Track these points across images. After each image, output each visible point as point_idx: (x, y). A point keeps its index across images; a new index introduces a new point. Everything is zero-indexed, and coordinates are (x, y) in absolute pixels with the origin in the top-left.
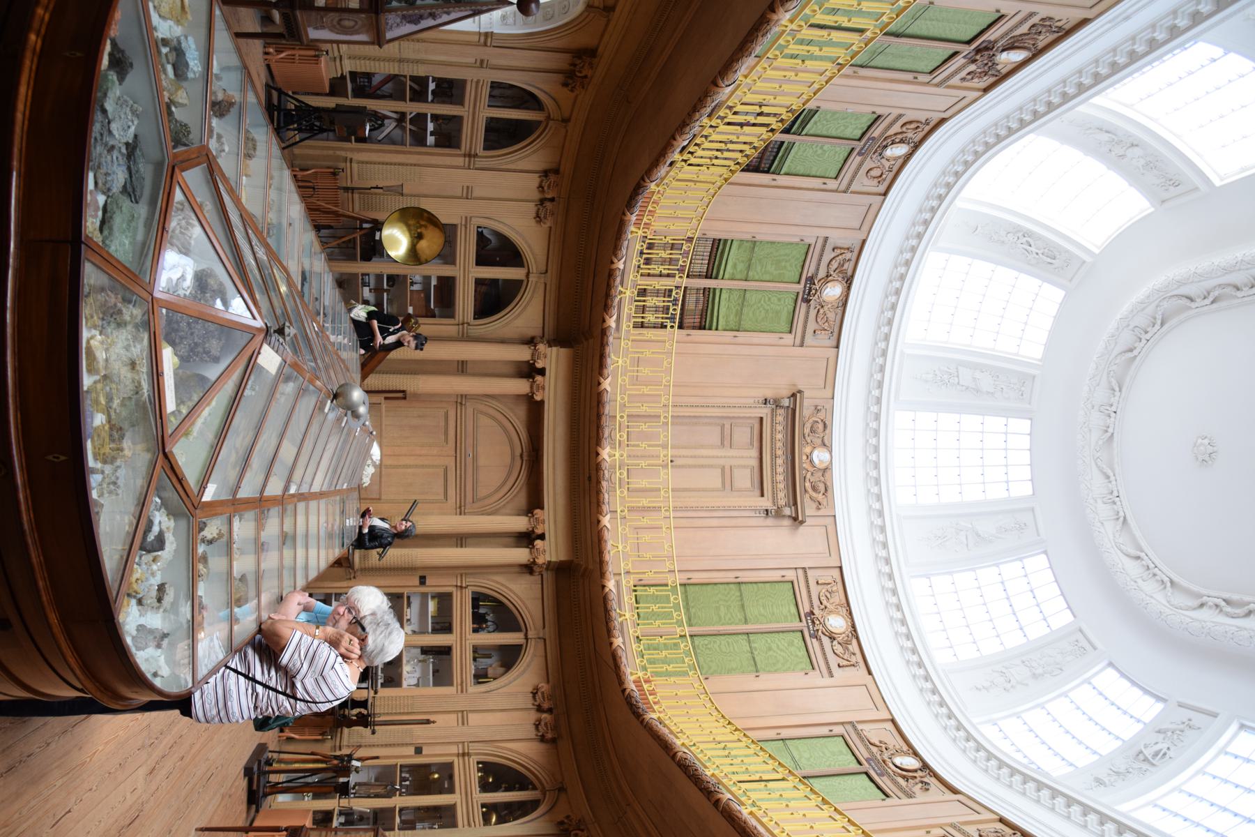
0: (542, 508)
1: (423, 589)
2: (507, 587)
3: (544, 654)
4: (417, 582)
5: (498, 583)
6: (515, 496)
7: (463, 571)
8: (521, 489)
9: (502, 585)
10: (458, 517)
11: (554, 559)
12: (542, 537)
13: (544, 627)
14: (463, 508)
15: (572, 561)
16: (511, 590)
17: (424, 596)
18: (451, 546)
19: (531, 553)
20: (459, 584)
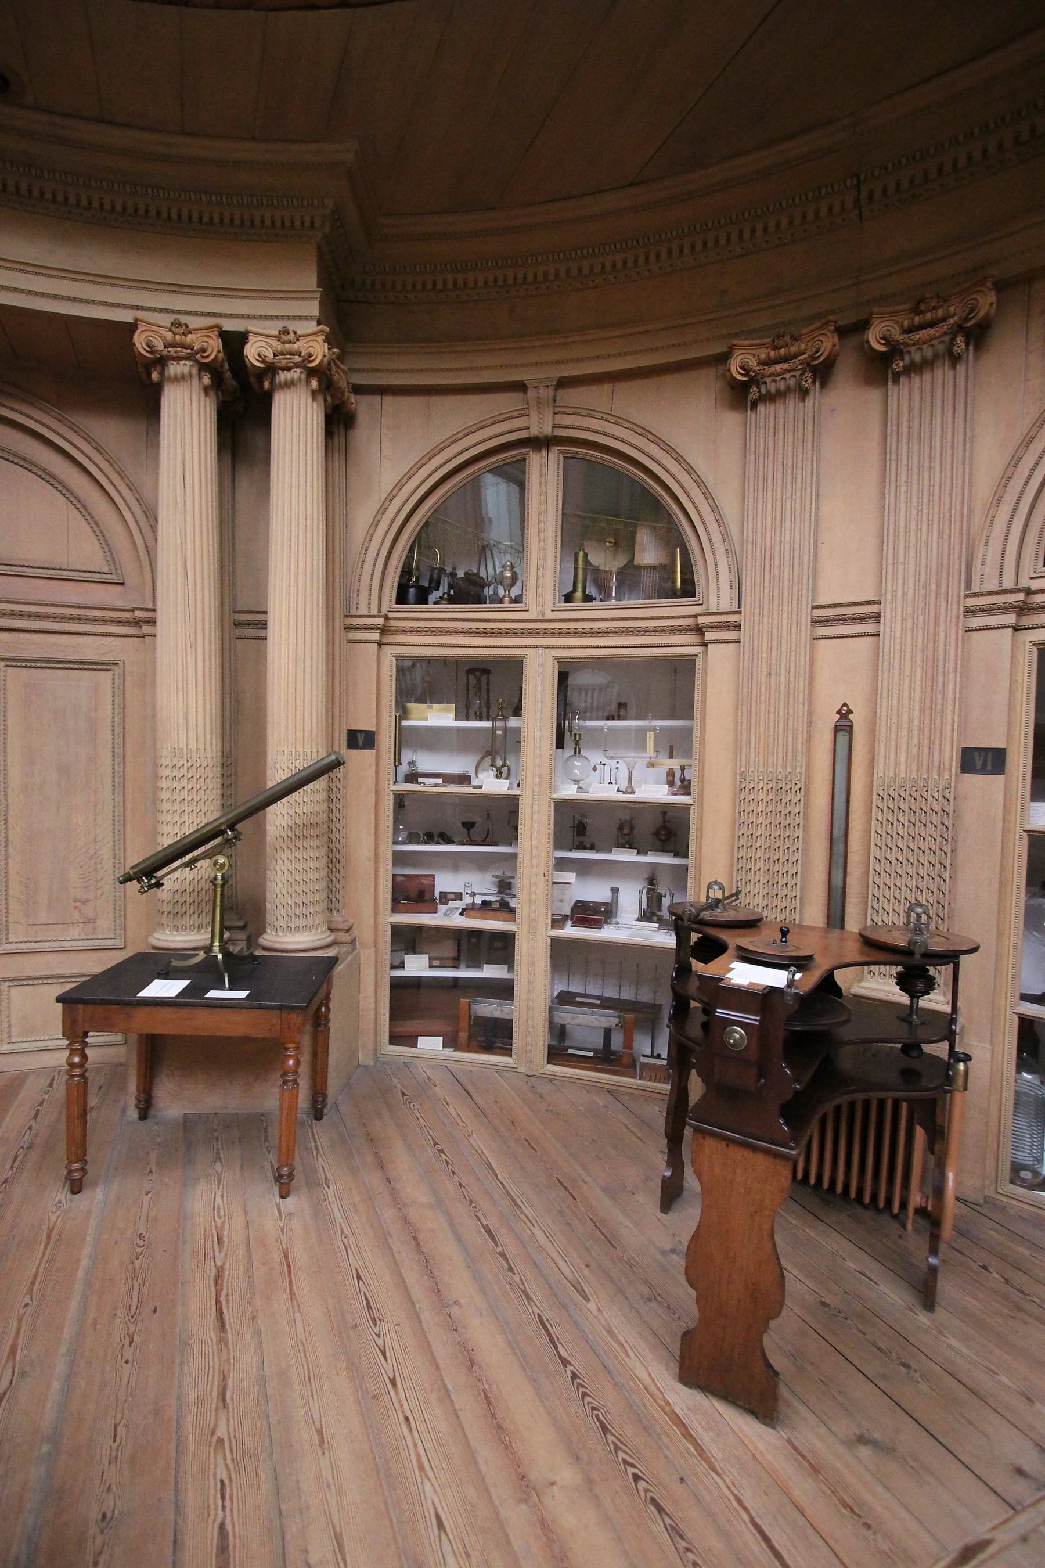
0: (131, 328)
1: (386, 740)
2: (390, 498)
3: (606, 387)
4: (368, 754)
5: (375, 524)
6: (98, 449)
7: (338, 624)
8: (87, 439)
9: (383, 510)
10: (160, 629)
11: (313, 308)
12: (234, 342)
13: (520, 387)
14: (138, 614)
15: (319, 248)
16: (399, 486)
17: (404, 738)
18: (261, 659)
19: (289, 384)
20: (376, 636)
